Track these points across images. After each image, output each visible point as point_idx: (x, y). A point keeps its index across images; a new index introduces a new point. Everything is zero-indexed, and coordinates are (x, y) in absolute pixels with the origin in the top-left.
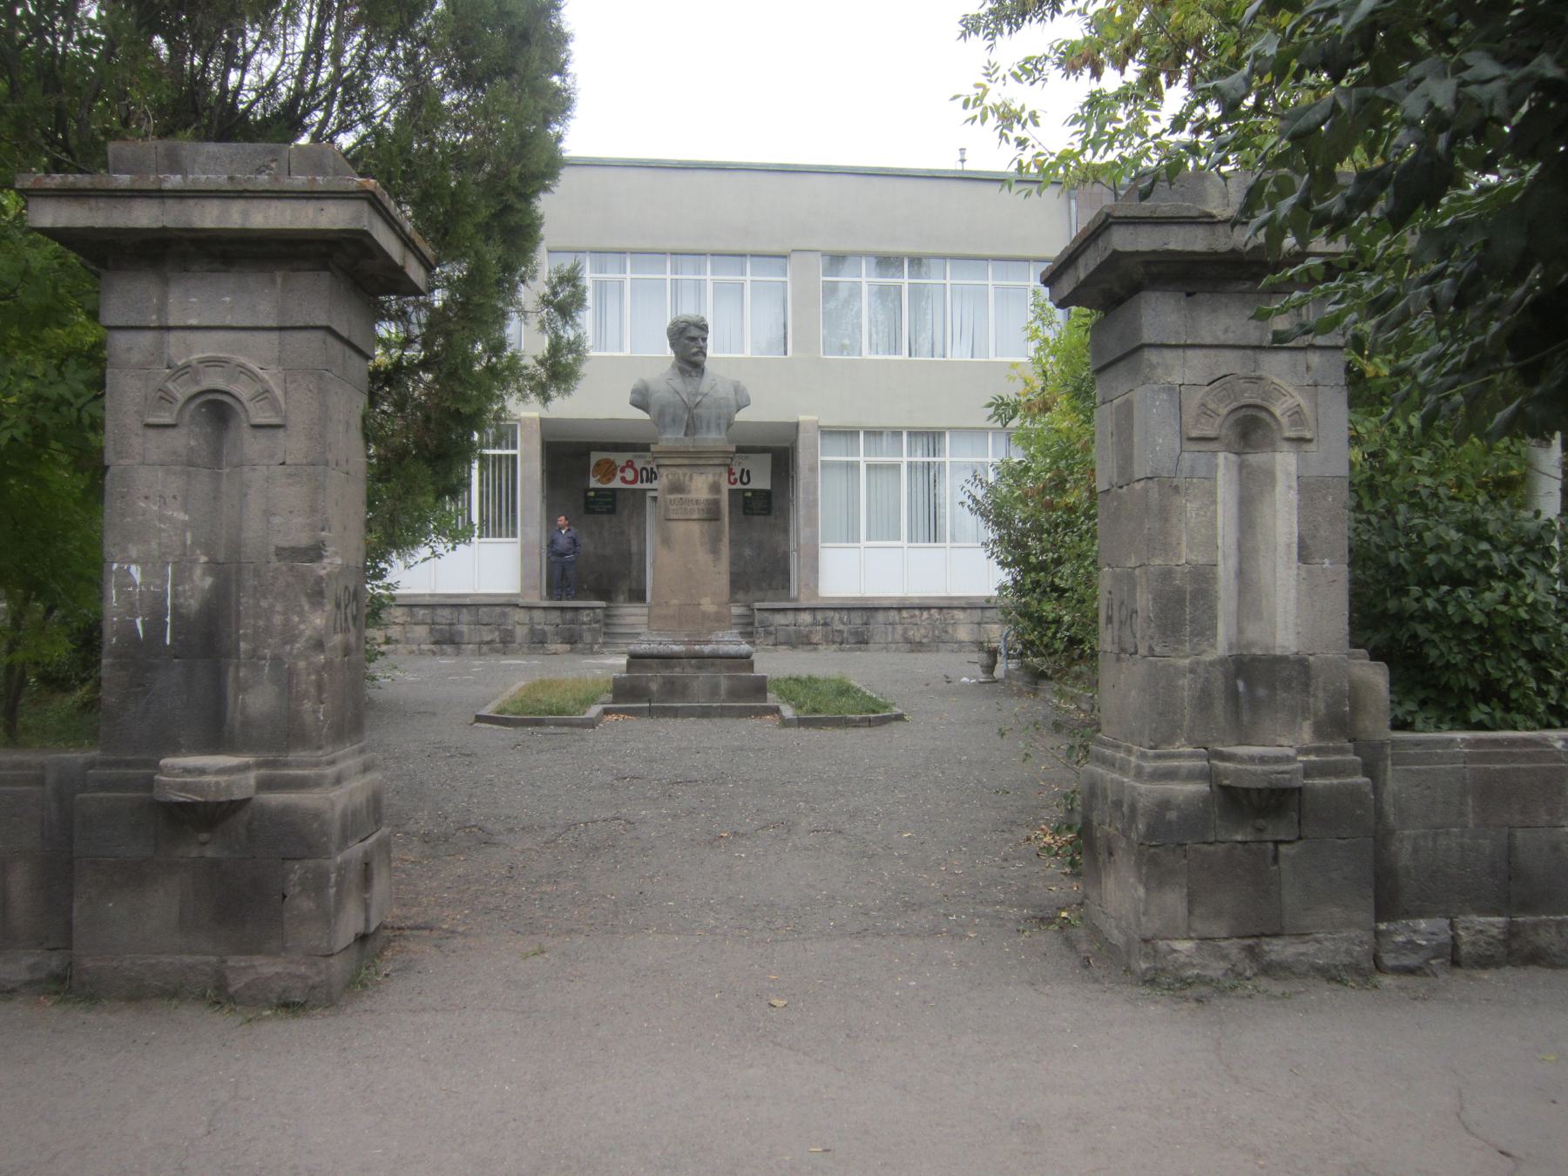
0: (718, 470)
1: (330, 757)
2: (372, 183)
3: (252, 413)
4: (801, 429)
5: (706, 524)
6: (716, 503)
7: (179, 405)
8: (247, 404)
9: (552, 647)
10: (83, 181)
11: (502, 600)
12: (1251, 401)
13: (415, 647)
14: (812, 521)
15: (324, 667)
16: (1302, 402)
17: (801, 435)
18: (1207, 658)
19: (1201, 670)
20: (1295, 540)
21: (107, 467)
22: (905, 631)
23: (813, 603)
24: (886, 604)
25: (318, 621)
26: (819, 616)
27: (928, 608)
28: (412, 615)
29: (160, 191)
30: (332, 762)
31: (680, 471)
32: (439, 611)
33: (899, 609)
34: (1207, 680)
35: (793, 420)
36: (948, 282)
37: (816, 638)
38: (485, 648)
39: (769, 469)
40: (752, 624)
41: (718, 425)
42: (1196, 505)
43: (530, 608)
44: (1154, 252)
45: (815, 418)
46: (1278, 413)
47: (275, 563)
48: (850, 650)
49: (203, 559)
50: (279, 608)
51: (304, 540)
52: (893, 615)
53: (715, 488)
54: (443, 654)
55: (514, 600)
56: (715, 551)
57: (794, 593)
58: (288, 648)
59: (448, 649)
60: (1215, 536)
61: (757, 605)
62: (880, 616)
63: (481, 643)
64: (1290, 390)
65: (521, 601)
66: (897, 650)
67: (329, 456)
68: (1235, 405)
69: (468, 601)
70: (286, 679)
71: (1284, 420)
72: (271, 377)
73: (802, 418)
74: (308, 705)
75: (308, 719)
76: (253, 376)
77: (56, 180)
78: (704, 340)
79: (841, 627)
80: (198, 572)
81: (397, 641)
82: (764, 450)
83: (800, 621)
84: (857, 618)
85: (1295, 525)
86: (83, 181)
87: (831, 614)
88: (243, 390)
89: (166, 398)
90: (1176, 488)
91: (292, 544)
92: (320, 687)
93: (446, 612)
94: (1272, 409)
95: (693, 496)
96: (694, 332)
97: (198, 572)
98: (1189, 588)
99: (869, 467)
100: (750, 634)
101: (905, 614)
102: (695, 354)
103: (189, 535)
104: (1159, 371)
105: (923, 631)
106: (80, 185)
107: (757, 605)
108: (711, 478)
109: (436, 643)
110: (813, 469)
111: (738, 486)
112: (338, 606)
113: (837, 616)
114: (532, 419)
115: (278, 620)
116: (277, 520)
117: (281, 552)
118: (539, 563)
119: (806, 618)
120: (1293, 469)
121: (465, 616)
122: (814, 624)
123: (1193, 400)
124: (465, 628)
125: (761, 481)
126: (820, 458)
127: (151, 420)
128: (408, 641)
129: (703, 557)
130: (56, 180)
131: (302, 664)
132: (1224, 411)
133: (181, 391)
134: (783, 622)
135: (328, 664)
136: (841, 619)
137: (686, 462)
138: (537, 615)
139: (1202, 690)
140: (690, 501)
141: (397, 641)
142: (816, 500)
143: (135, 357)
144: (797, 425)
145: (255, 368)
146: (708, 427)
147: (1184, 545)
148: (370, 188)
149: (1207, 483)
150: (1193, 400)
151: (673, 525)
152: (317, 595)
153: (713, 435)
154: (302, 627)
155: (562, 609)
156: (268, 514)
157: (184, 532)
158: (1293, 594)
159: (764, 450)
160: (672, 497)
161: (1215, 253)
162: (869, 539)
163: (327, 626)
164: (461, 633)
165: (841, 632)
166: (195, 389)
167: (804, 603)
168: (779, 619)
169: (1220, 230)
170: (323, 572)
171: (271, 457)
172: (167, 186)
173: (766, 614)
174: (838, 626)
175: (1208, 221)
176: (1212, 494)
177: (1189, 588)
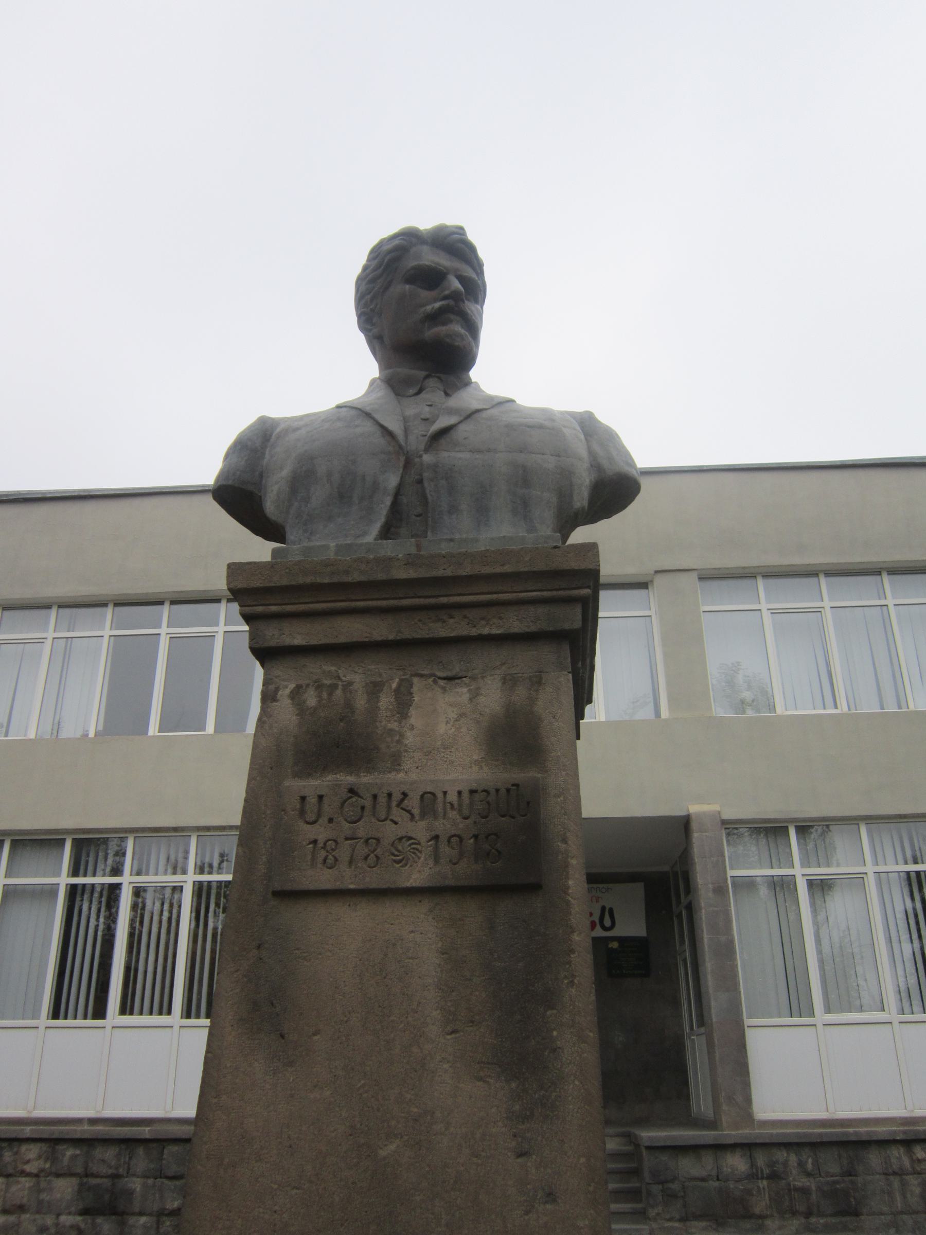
0: (523, 660)
4: (694, 825)
5: (473, 914)
14: (729, 981)
17: (696, 836)
24: (882, 1131)
26: (761, 1160)
28: (54, 1159)
31: (355, 675)
32: (99, 1152)
35: (678, 811)
36: (890, 601)
37: (760, 1205)
39: (643, 907)
40: (636, 1172)
45: (715, 807)
52: (897, 1155)
56: (520, 1058)
57: (702, 1104)
62: (874, 1158)
63: (161, 1214)
69: (146, 1132)
73: (694, 809)
79: (802, 1182)
81: (21, 1208)
82: (633, 878)
83: (726, 1170)
84: (832, 1165)
87: (781, 1155)
93: (109, 1154)
95: (412, 775)
96: (430, 258)
99: (811, 884)
100: (634, 1195)
102: (435, 318)
107: (647, 1135)
108: (493, 697)
109: (85, 1212)
110: (720, 890)
111: (599, 932)
113: (793, 1159)
119: (737, 1163)
121: (141, 1161)
122: (754, 1175)
124: (136, 1184)
125: (631, 925)
126: (731, 873)
128: (41, 1208)
129: (460, 1098)
134: (696, 1171)
136: (801, 1165)
137: (380, 629)
142: (732, 942)
144: (685, 824)
146: (482, 512)
151: (315, 920)
159: (633, 878)
160: (312, 785)
162: (828, 1010)
164: (130, 1193)
165: (805, 1191)
167: (729, 1133)
168: (688, 1167)
173: (664, 1157)
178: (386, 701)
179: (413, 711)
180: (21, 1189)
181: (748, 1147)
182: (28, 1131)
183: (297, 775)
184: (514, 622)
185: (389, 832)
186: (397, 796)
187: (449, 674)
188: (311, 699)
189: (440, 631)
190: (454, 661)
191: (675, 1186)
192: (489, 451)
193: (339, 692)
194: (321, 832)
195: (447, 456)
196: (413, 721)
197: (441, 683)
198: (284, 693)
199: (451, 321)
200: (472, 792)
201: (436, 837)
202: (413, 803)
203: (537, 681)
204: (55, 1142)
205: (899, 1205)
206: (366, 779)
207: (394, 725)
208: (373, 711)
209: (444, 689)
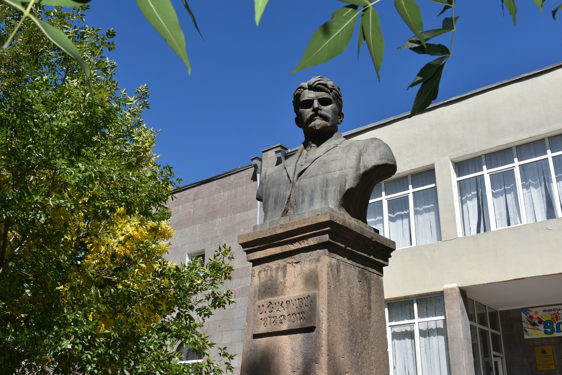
53: (311, 279)
114: (452, 289)
146: (312, 200)
160: (260, 302)
178: (280, 273)
179: (287, 275)
183: (259, 299)
184: (312, 242)
185: (279, 314)
186: (280, 303)
187: (296, 261)
188: (263, 274)
189: (292, 247)
190: (297, 257)
192: (316, 175)
193: (269, 271)
194: (263, 316)
195: (304, 181)
196: (287, 278)
197: (294, 264)
198: (256, 273)
199: (316, 119)
200: (298, 299)
201: (289, 315)
202: (285, 305)
203: (318, 260)
206: (275, 298)
207: (282, 280)
208: (277, 276)
209: (295, 267)
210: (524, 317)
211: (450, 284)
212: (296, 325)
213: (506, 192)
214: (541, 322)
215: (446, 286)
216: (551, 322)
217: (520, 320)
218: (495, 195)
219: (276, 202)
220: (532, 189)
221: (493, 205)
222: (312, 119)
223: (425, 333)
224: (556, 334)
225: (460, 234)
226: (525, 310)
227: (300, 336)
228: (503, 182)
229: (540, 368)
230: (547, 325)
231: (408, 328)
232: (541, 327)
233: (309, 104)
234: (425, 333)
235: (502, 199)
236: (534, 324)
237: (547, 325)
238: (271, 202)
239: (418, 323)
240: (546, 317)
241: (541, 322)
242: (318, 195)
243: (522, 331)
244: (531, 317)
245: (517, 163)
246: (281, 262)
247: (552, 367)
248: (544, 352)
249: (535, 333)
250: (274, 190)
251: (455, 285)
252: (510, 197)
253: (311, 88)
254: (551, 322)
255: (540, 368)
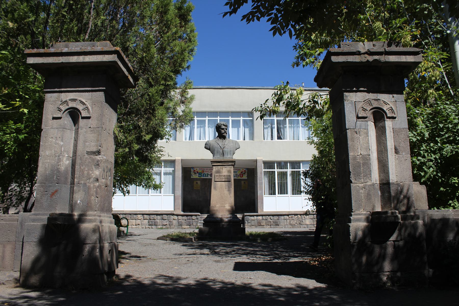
1: (99, 214)
2: (118, 49)
3: (82, 114)
6: (230, 176)
7: (63, 111)
8: (82, 111)
9: (184, 227)
10: (42, 51)
11: (169, 213)
12: (376, 106)
13: (144, 226)
15: (98, 187)
16: (392, 106)
18: (369, 183)
19: (367, 187)
20: (394, 147)
21: (42, 130)
22: (290, 221)
23: (262, 213)
24: (284, 213)
25: (97, 173)
27: (297, 215)
29: (62, 53)
30: (100, 216)
33: (288, 215)
34: (369, 190)
38: (164, 227)
41: (230, 154)
42: (362, 137)
43: (177, 215)
44: (344, 62)
46: (385, 109)
47: (86, 156)
48: (274, 227)
49: (66, 155)
50: (86, 169)
51: (95, 149)
53: (229, 171)
54: (152, 228)
55: (173, 213)
56: (229, 190)
58: (88, 181)
59: (153, 227)
60: (369, 146)
61: (245, 214)
62: (282, 217)
64: (388, 103)
65: (175, 213)
66: (288, 227)
67: (103, 126)
68: (371, 107)
69: (159, 213)
70: (87, 190)
71: (387, 111)
72: (88, 104)
73: (258, 158)
74: (93, 198)
75: (93, 202)
76: (83, 104)
77: (35, 51)
78: (226, 129)
80: (65, 159)
84: (276, 218)
85: (393, 143)
86: (42, 51)
88: (80, 107)
89: (60, 110)
90: (356, 132)
91: (91, 150)
92: (96, 192)
94: (383, 108)
97: (65, 159)
98: (361, 162)
101: (290, 216)
103: (63, 148)
104: (349, 98)
105: (295, 221)
106: (41, 52)
112: (104, 171)
115: (86, 172)
116: (87, 144)
117: (88, 153)
118: (180, 202)
120: (391, 126)
123: (359, 106)
124: (158, 221)
127: (55, 116)
129: (226, 192)
130: (35, 51)
131: (92, 185)
132: (369, 109)
133: (64, 108)
135: (99, 187)
137: (221, 164)
138: (180, 217)
139: (368, 194)
140: (221, 176)
141: (139, 225)
143: (52, 99)
144: (256, 161)
145: (84, 101)
146: (227, 154)
147: (359, 149)
148: (118, 50)
149: (365, 130)
150: (359, 106)
152: (98, 165)
153: (229, 156)
154: (92, 175)
155: (187, 216)
156: (85, 142)
157: (61, 147)
158: (394, 163)
161: (362, 62)
163: (100, 175)
165: (271, 222)
166: (67, 107)
167: (259, 213)
169: (362, 55)
170: (99, 159)
171: (87, 126)
172: (64, 51)
174: (269, 220)
175: (359, 53)
176: (367, 134)
177: (361, 162)
180: (138, 222)
181: (262, 215)
182: (138, 213)
184: (230, 164)
191: (250, 221)
204: (143, 214)
205: (285, 224)
210: (192, 170)
211: (178, 157)
212: (226, 180)
213: (201, 127)
214: (198, 172)
215: (176, 158)
216: (201, 173)
217: (191, 171)
218: (197, 127)
219: (217, 152)
220: (210, 128)
221: (196, 131)
222: (224, 133)
223: (165, 174)
224: (202, 177)
225: (184, 140)
226: (193, 168)
227: (227, 182)
228: (202, 123)
229: (195, 188)
230: (200, 174)
231: (158, 171)
232: (198, 174)
233: (223, 129)
234: (165, 174)
235: (199, 129)
236: (195, 173)
237: (200, 174)
238: (216, 152)
239: (163, 170)
240: (200, 171)
241: (198, 172)
242: (229, 153)
243: (190, 175)
244: (195, 171)
245: (207, 118)
246: (221, 167)
247: (199, 188)
248: (197, 183)
249: (194, 176)
250: (216, 149)
251: (180, 158)
252: (202, 129)
253: (224, 125)
254: (201, 173)
255: (195, 188)
